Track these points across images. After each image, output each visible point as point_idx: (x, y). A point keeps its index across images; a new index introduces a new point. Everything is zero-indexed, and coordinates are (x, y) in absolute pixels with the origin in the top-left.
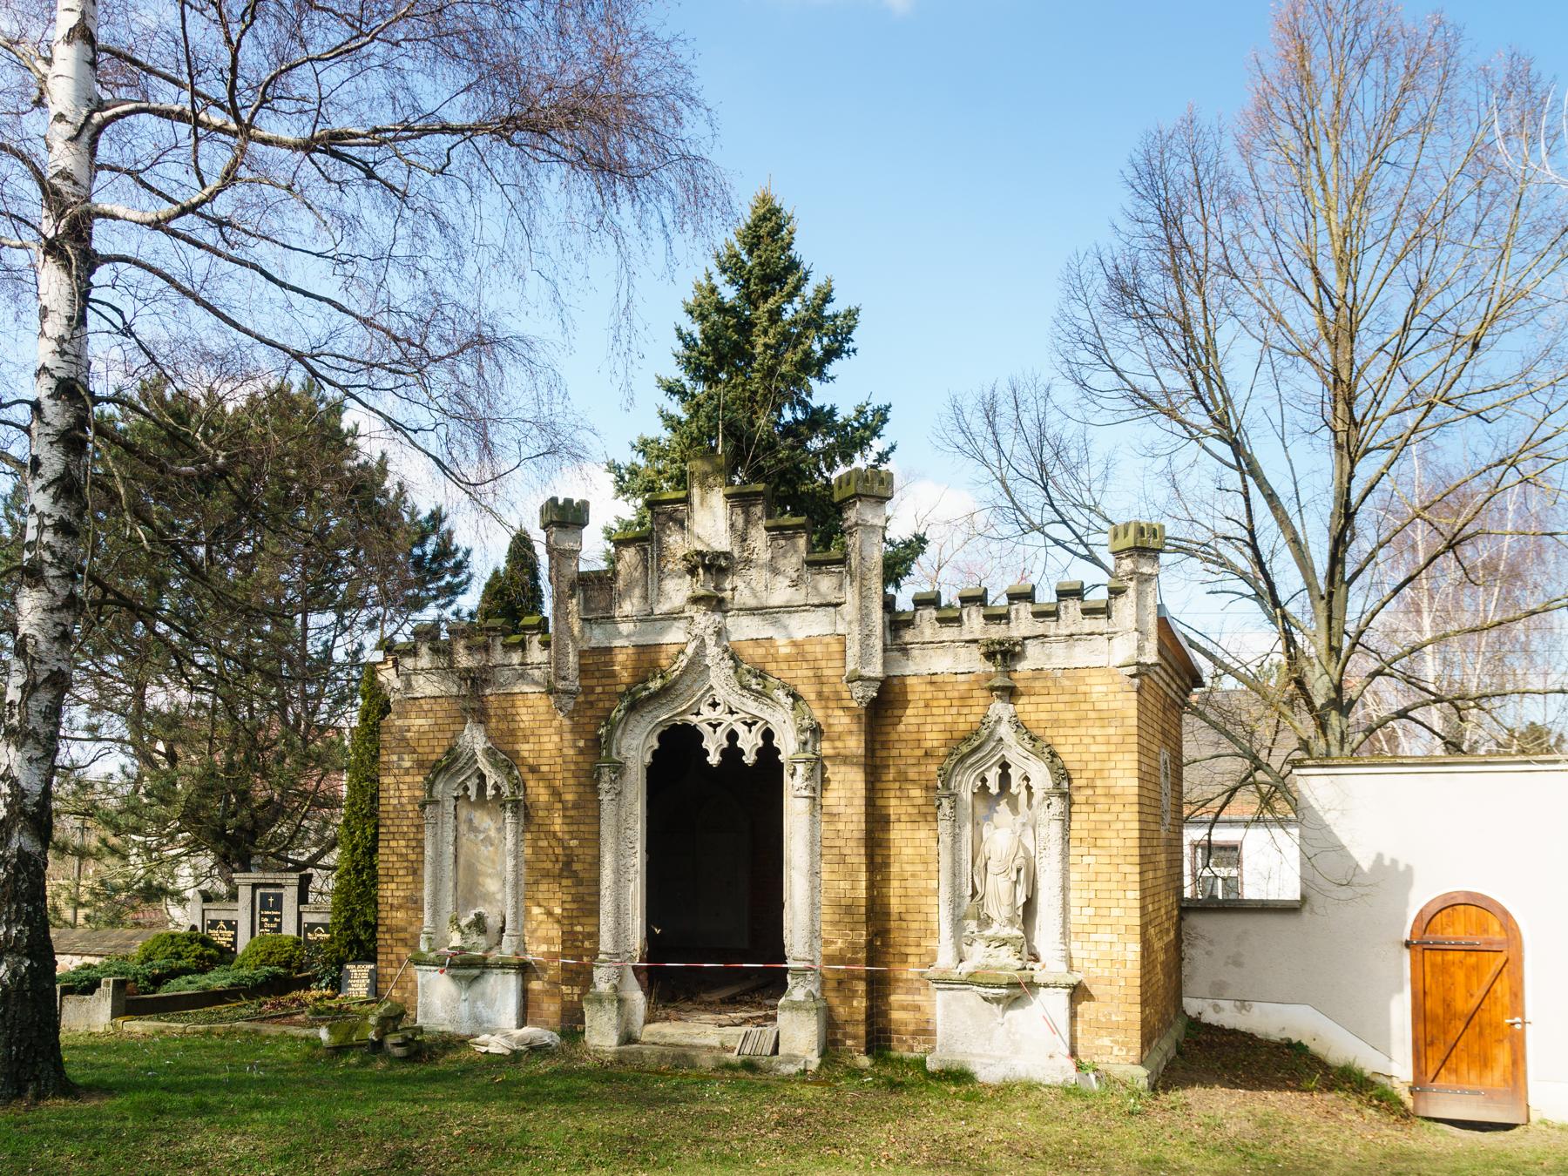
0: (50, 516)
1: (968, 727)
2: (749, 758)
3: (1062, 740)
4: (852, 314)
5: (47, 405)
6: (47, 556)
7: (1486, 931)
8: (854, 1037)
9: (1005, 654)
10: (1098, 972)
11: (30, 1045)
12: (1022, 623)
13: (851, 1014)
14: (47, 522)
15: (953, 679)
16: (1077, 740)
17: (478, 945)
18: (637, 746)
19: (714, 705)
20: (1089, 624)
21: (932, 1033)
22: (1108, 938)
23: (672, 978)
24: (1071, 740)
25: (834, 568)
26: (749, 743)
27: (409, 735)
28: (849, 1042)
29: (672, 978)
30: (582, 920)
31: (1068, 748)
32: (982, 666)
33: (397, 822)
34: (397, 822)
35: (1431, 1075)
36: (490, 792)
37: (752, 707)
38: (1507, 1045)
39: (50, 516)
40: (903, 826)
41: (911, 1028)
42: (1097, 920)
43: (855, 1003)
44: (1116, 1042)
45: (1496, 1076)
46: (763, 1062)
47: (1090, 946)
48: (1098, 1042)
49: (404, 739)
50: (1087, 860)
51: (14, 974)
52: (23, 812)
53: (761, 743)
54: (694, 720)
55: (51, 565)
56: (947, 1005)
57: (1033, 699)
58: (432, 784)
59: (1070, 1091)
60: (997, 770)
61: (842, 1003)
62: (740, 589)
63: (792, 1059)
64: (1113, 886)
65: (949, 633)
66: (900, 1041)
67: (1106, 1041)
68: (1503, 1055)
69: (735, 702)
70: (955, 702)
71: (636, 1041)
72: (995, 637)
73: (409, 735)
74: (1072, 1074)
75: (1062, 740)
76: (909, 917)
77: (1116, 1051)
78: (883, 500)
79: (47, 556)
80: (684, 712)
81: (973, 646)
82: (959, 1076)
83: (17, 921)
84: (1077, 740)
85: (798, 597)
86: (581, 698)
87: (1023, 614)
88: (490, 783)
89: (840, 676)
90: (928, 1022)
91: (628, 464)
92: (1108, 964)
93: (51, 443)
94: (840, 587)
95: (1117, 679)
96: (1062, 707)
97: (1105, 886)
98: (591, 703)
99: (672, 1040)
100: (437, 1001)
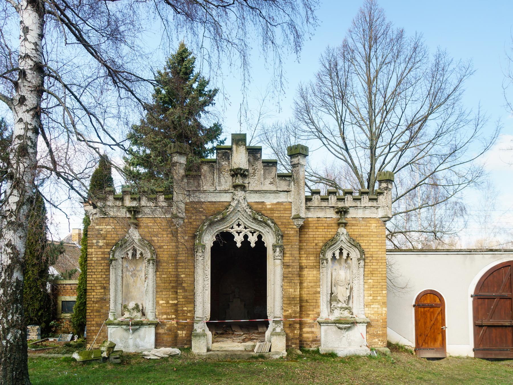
0: (31, 124)
1: (330, 236)
2: (253, 245)
3: (362, 241)
4: (216, 91)
5: (28, 72)
6: (29, 143)
7: (435, 301)
8: (296, 344)
9: (342, 212)
10: (374, 317)
11: (21, 370)
12: (349, 202)
13: (294, 336)
14: (30, 127)
15: (325, 219)
16: (367, 241)
17: (138, 316)
18: (209, 240)
19: (239, 225)
20: (370, 204)
21: (319, 341)
22: (376, 306)
23: (219, 325)
24: (365, 241)
25: (288, 179)
26: (253, 240)
27: (102, 232)
28: (293, 346)
29: (219, 325)
30: (186, 305)
31: (364, 244)
32: (335, 216)
33: (96, 267)
34: (96, 267)
35: (421, 345)
36: (138, 256)
37: (255, 226)
38: (441, 334)
39: (31, 124)
40: (307, 270)
41: (311, 339)
42: (373, 301)
43: (296, 332)
44: (379, 340)
45: (438, 344)
46: (266, 355)
47: (371, 309)
48: (374, 341)
49: (100, 234)
50: (370, 281)
51: (15, 338)
52: (18, 261)
53: (243, 240)
54: (231, 231)
55: (31, 147)
56: (326, 331)
57: (353, 227)
58: (114, 252)
59: (370, 357)
60: (338, 251)
61: (291, 332)
62: (253, 183)
63: (277, 353)
64: (378, 289)
65: (324, 204)
66: (307, 344)
67: (376, 340)
68: (440, 337)
69: (248, 224)
70: (326, 228)
71: (211, 351)
72: (340, 206)
73: (102, 232)
74: (369, 352)
75: (362, 241)
76: (310, 301)
77: (379, 343)
78: (306, 156)
79: (29, 143)
80: (227, 227)
81: (332, 209)
82: (332, 355)
83: (16, 312)
84: (367, 241)
85: (273, 188)
86: (186, 221)
87: (349, 199)
88: (138, 253)
89: (290, 217)
90: (317, 337)
91: (427, 132)
92: (377, 315)
93: (31, 91)
94: (289, 185)
95: (380, 222)
96: (362, 230)
97: (376, 289)
98: (191, 222)
99: (225, 349)
100: (120, 339)
